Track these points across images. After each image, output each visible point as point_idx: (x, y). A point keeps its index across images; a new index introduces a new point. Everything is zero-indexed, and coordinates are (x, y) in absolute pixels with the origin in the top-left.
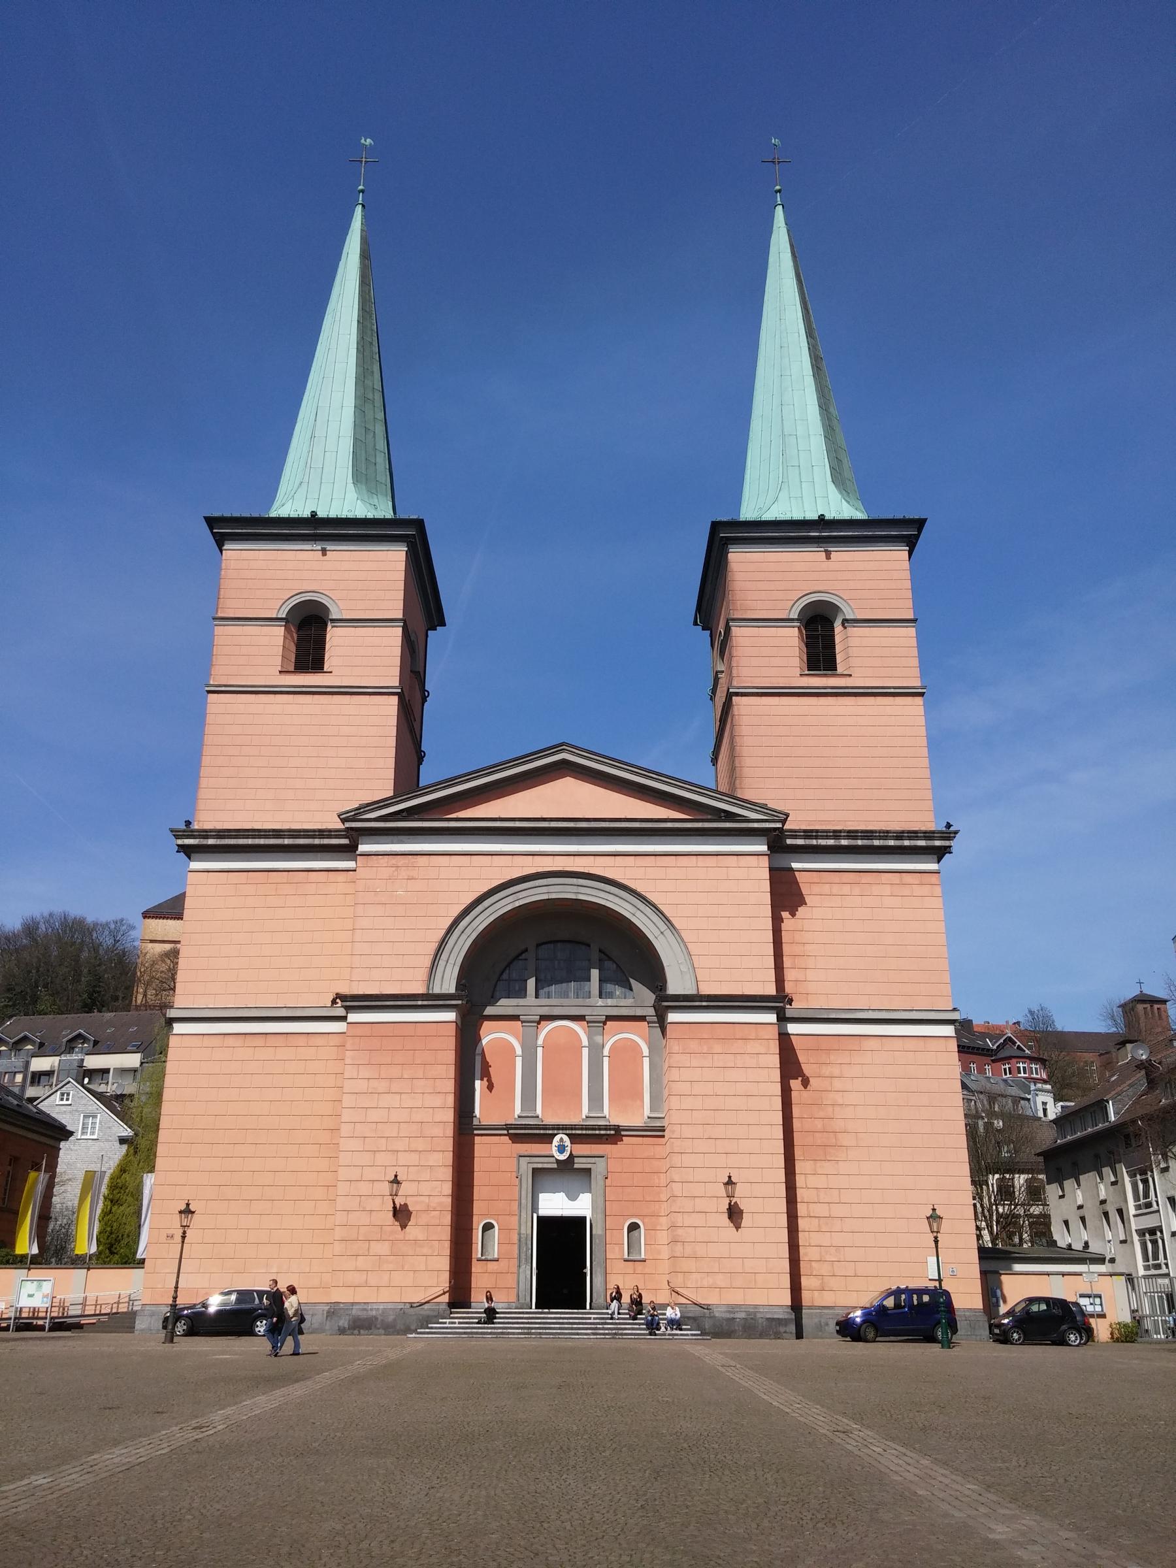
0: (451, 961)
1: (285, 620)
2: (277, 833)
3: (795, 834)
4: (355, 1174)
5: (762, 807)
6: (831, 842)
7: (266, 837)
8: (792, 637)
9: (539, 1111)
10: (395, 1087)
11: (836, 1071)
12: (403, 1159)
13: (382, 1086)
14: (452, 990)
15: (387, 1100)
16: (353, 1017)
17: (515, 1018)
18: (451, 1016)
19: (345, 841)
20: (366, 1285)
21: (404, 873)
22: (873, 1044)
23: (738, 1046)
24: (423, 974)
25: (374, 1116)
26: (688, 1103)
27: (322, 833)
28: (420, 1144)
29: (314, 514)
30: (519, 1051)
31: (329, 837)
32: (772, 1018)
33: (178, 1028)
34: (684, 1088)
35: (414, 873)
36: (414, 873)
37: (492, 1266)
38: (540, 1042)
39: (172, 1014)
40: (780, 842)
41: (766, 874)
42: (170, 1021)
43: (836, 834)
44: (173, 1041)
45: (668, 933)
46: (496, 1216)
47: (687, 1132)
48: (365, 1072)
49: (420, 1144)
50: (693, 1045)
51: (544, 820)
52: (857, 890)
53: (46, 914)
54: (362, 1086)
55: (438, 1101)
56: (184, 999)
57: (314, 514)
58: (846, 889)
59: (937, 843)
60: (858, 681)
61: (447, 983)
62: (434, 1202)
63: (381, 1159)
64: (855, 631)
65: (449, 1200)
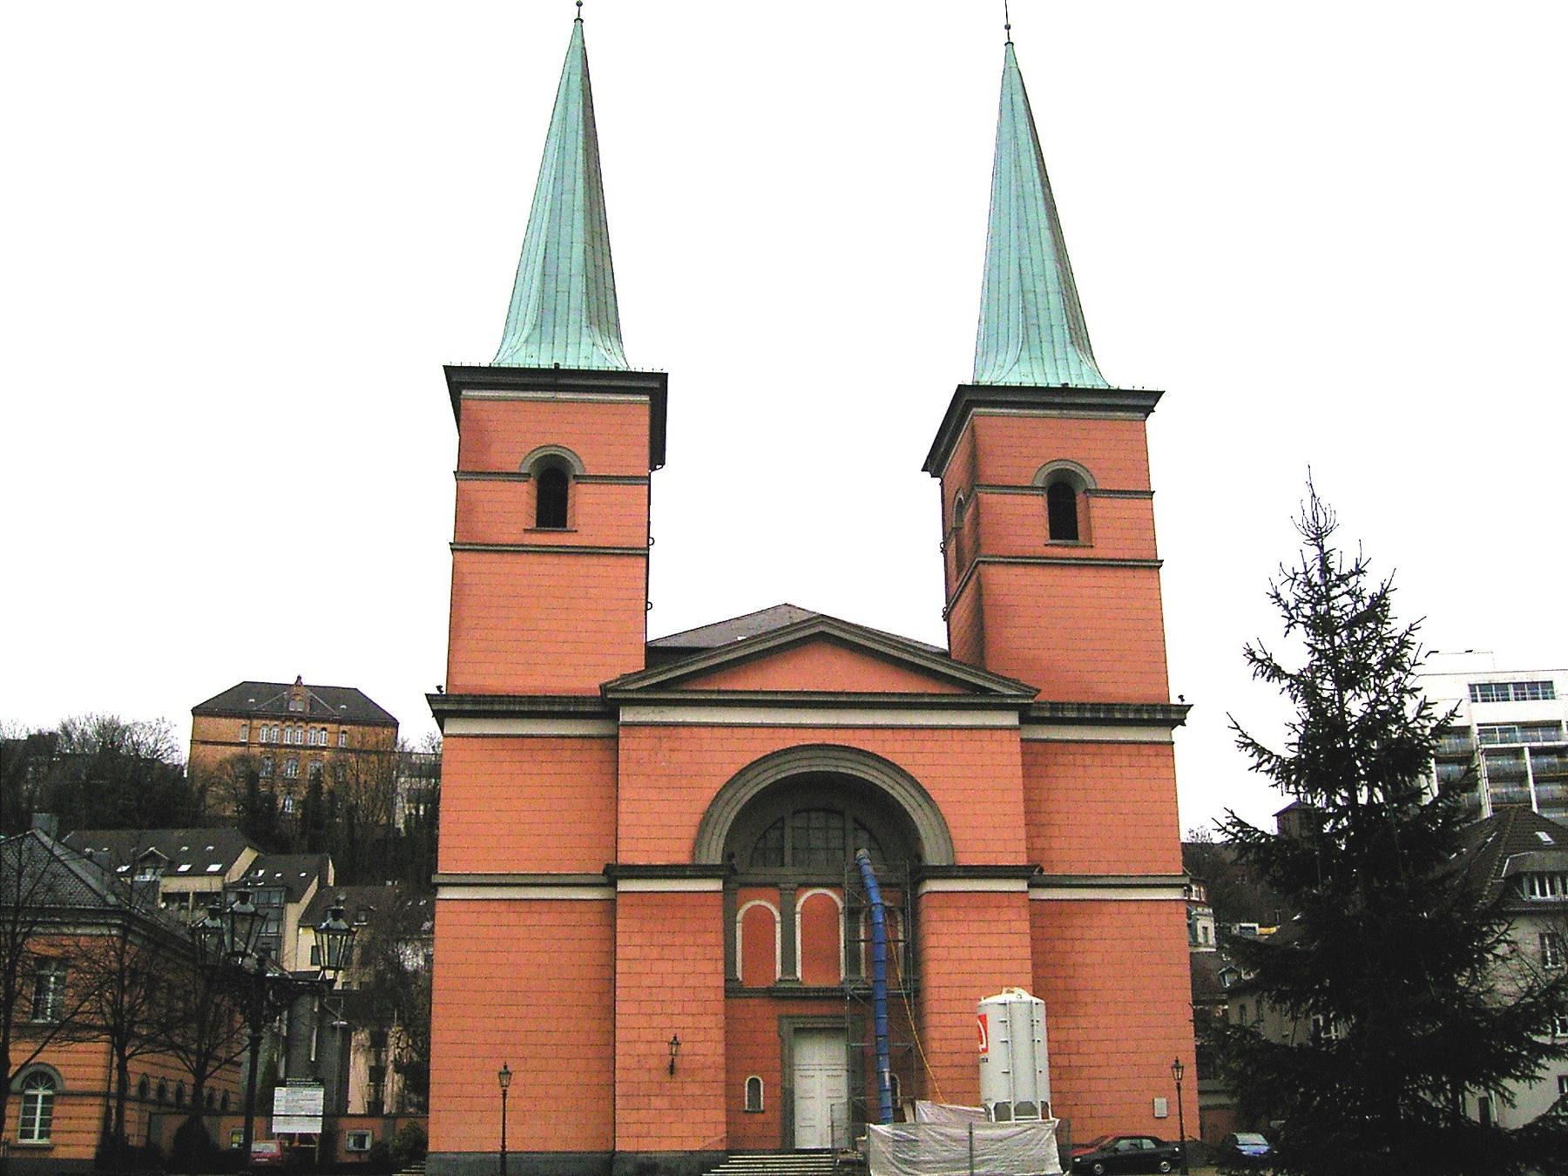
0: (717, 832)
1: (529, 475)
2: (532, 699)
3: (1040, 706)
4: (632, 1035)
5: (1015, 683)
6: (1074, 715)
7: (521, 703)
8: (1038, 505)
9: (799, 975)
10: (667, 953)
11: (1077, 934)
12: (677, 1020)
13: (655, 953)
14: (719, 862)
15: (660, 967)
16: (623, 886)
17: (774, 885)
18: (715, 885)
19: (597, 709)
20: (648, 1135)
21: (666, 744)
22: (1113, 907)
23: (992, 913)
24: (687, 845)
25: (647, 981)
26: (946, 967)
27: (577, 700)
28: (694, 1008)
29: (557, 365)
30: (778, 919)
31: (584, 704)
32: (1021, 885)
33: (444, 893)
34: (941, 953)
35: (676, 745)
36: (676, 745)
37: (759, 1117)
38: (798, 909)
39: (436, 879)
40: (1028, 717)
41: (1016, 747)
42: (436, 886)
43: (1080, 707)
44: (439, 907)
45: (925, 805)
46: (761, 1073)
47: (945, 993)
48: (637, 940)
49: (694, 1008)
50: (951, 913)
51: (805, 693)
52: (1098, 760)
53: (108, 717)
54: (636, 952)
55: (709, 967)
56: (447, 863)
57: (557, 365)
58: (1088, 761)
59: (1174, 716)
60: (1100, 551)
61: (714, 856)
62: (710, 1060)
63: (656, 1021)
64: (1095, 502)
65: (722, 1060)
